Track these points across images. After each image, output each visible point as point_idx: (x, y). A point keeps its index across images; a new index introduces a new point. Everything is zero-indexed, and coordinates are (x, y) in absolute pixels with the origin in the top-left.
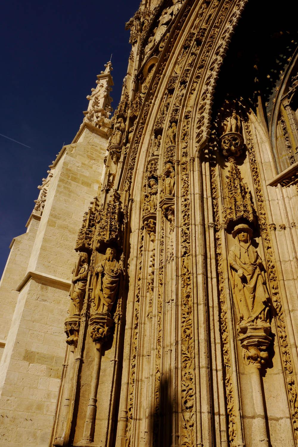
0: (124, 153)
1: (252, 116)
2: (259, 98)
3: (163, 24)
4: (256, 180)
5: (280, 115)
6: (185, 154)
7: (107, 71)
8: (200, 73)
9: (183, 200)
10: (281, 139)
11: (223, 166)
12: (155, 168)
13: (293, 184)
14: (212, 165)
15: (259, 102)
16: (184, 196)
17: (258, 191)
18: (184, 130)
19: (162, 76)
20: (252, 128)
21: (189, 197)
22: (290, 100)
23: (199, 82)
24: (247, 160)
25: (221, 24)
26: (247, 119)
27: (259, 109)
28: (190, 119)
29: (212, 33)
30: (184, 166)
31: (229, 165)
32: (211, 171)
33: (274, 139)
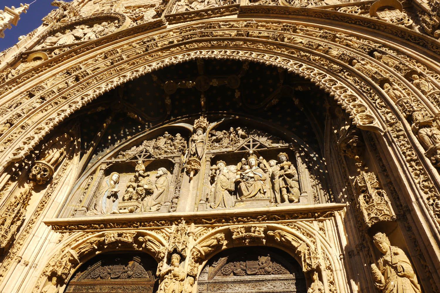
1: (76, 158)
2: (91, 149)
3: (73, 35)
4: (37, 213)
5: (94, 172)
7: (18, 11)
8: (60, 102)
10: (81, 190)
11: (21, 185)
13: (60, 232)
14: (12, 179)
15: (89, 152)
17: (32, 222)
18: (12, 136)
19: (36, 75)
20: (69, 168)
22: (107, 167)
23: (54, 107)
24: (43, 192)
25: (100, 81)
26: (70, 158)
27: (86, 156)
28: (24, 131)
29: (90, 81)
31: (27, 186)
32: (7, 183)
33: (77, 187)
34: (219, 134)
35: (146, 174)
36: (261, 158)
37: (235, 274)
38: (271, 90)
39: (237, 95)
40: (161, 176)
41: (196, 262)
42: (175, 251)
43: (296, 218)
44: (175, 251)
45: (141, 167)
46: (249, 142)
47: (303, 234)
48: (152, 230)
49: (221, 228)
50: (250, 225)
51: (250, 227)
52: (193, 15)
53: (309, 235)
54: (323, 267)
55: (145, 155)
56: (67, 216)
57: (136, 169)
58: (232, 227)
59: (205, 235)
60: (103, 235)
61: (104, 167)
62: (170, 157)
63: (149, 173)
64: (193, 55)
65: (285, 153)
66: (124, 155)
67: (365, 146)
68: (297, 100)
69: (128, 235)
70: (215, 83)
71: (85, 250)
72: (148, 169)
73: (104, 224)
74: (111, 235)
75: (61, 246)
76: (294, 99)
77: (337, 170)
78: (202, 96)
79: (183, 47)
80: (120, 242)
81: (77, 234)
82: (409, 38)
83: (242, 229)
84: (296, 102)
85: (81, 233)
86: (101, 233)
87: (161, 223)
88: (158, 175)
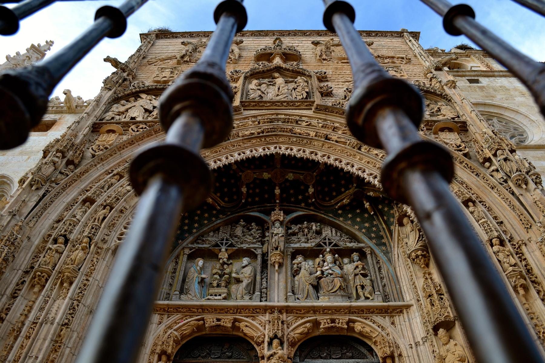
0: (46, 189)
5: (178, 257)
6: (104, 241)
9: (85, 278)
12: (71, 230)
16: (87, 275)
21: (91, 279)
28: (123, 215)
30: (99, 251)
34: (295, 228)
35: (229, 262)
36: (336, 255)
37: (322, 358)
38: (343, 190)
39: (311, 190)
40: (246, 266)
41: (291, 346)
42: (276, 337)
43: (372, 313)
44: (276, 337)
45: (224, 255)
46: (325, 239)
47: (379, 327)
48: (247, 317)
49: (309, 318)
50: (335, 317)
51: (335, 320)
52: (268, 104)
53: (383, 328)
54: (396, 355)
55: (226, 244)
56: (161, 299)
57: (220, 257)
58: (319, 318)
59: (297, 324)
60: (203, 319)
61: (187, 251)
62: (253, 248)
63: (231, 261)
64: (272, 150)
65: (357, 254)
66: (203, 241)
67: (429, 257)
68: (368, 204)
69: (227, 321)
70: (290, 176)
71: (186, 332)
72: (230, 257)
73: (202, 309)
74: (210, 320)
75: (163, 327)
76: (365, 202)
77: (404, 273)
78: (277, 188)
79: (263, 139)
80: (219, 325)
81: (175, 317)
82: (466, 166)
83: (328, 320)
84: (367, 205)
85: (179, 316)
86: (199, 317)
87: (256, 312)
88: (244, 265)
